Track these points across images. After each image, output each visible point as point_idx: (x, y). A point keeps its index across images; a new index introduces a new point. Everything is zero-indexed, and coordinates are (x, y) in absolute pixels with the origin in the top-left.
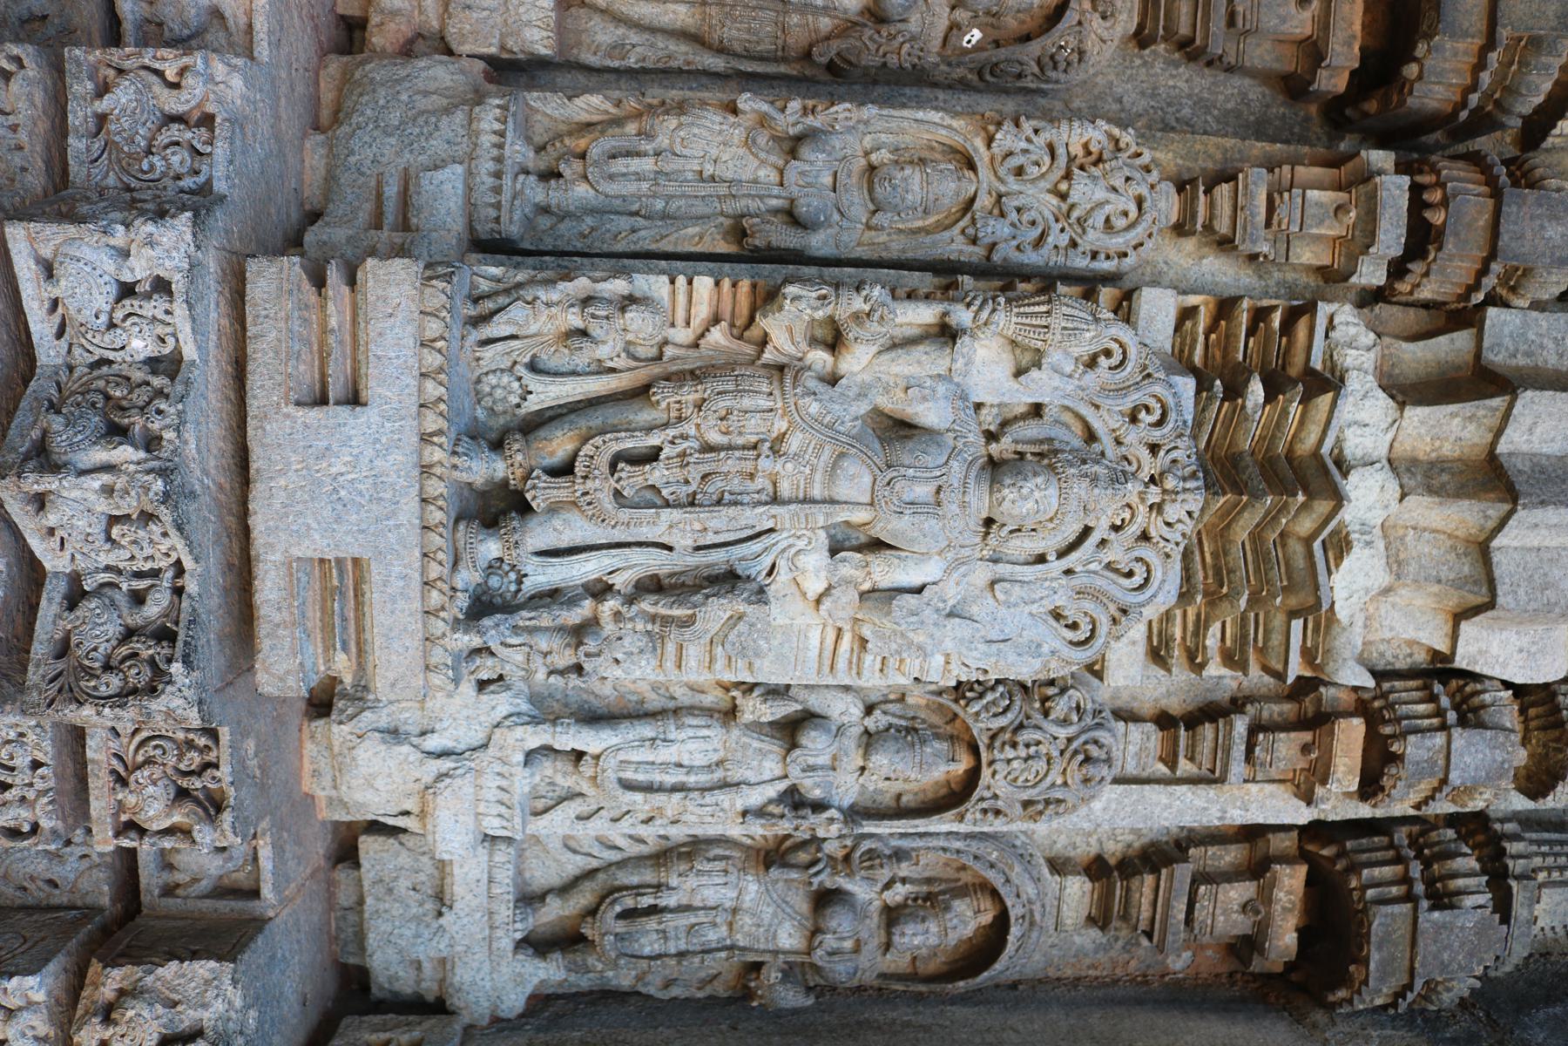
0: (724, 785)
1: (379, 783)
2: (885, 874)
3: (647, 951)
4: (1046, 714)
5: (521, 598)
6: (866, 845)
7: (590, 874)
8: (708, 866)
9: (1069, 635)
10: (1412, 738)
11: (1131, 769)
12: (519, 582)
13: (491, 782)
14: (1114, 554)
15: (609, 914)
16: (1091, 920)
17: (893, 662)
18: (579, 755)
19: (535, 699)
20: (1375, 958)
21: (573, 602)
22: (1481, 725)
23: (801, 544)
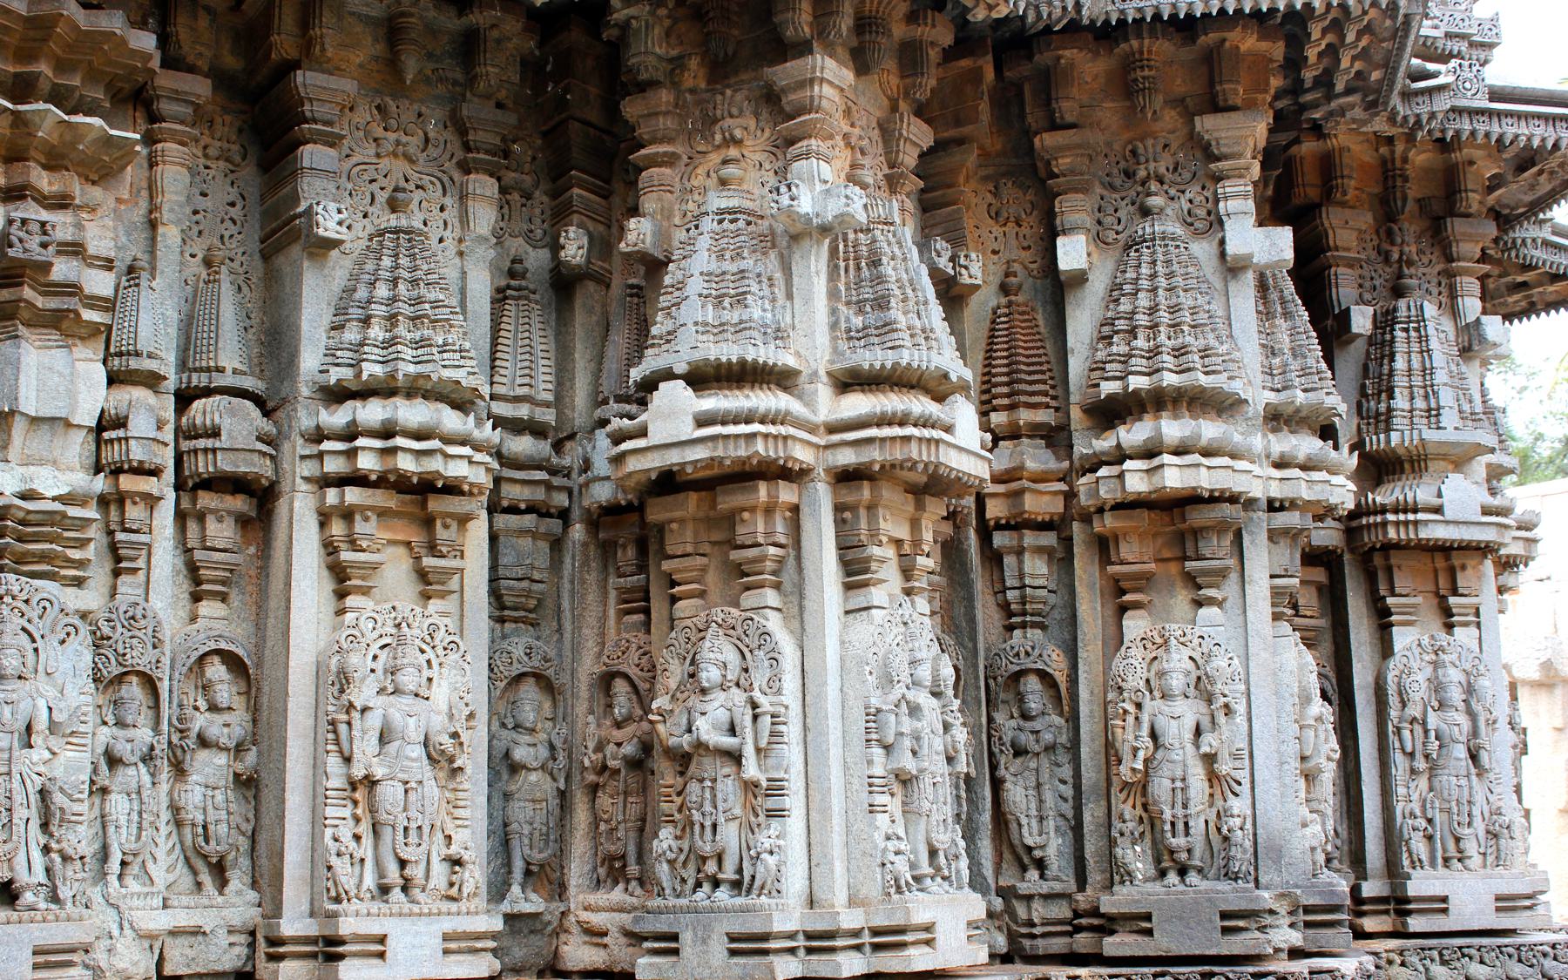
0: (139, 793)
1: (136, 959)
2: (189, 711)
3: (226, 830)
4: (109, 638)
5: (49, 884)
6: (175, 722)
7: (187, 859)
8: (183, 801)
9: (73, 636)
10: (131, 457)
11: (141, 591)
12: (42, 885)
13: (136, 902)
14: (34, 615)
15: (207, 849)
16: (223, 600)
17: (83, 718)
18: (123, 863)
19: (95, 884)
20: (243, 469)
21: (52, 861)
22: (127, 417)
23: (27, 762)
